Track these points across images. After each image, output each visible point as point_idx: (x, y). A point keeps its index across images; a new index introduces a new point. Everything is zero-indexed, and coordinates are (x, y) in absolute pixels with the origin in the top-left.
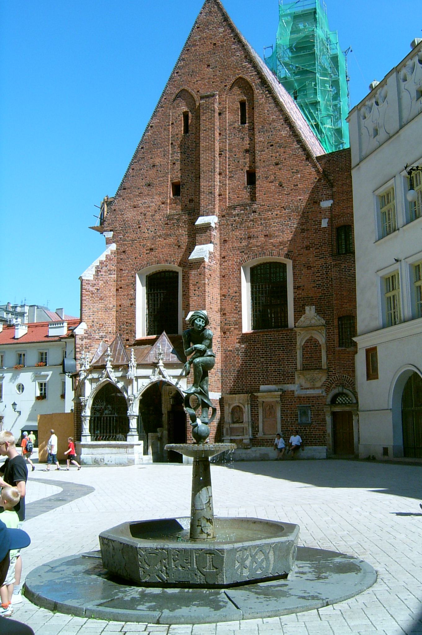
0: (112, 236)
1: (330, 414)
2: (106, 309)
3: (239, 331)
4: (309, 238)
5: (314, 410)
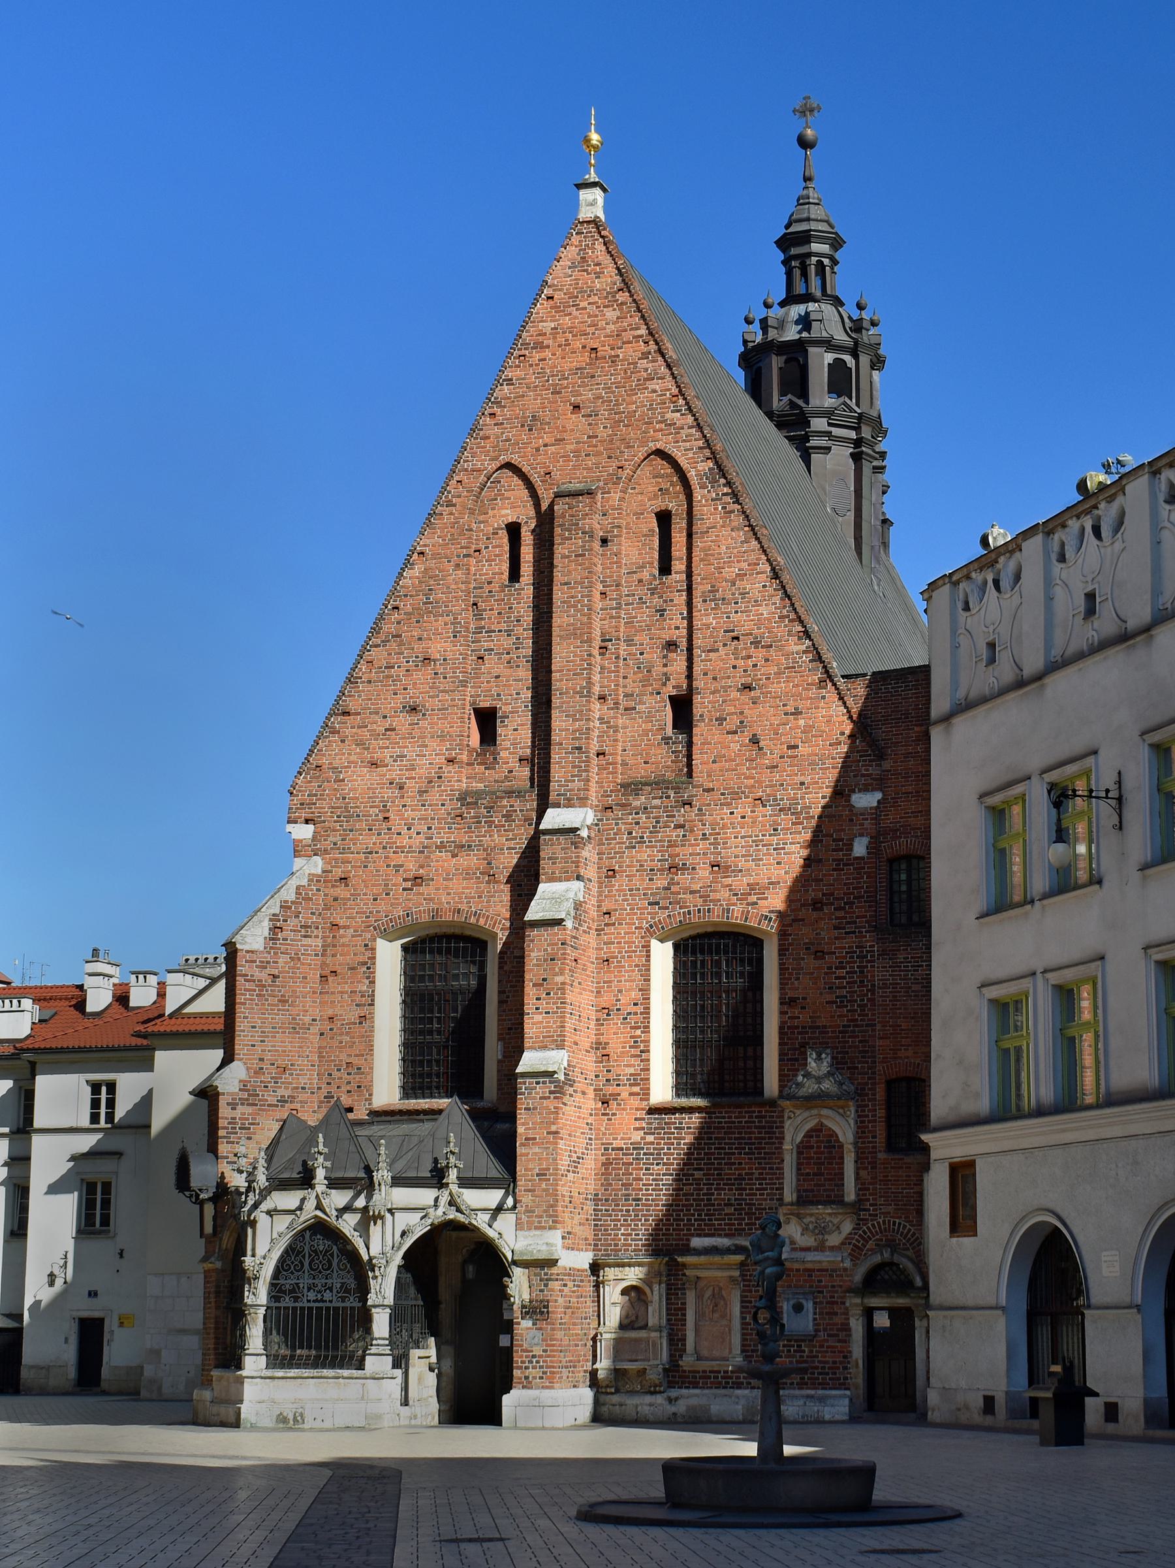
0: (310, 836)
1: (860, 1312)
2: (296, 1028)
3: (641, 1100)
5: (821, 1303)
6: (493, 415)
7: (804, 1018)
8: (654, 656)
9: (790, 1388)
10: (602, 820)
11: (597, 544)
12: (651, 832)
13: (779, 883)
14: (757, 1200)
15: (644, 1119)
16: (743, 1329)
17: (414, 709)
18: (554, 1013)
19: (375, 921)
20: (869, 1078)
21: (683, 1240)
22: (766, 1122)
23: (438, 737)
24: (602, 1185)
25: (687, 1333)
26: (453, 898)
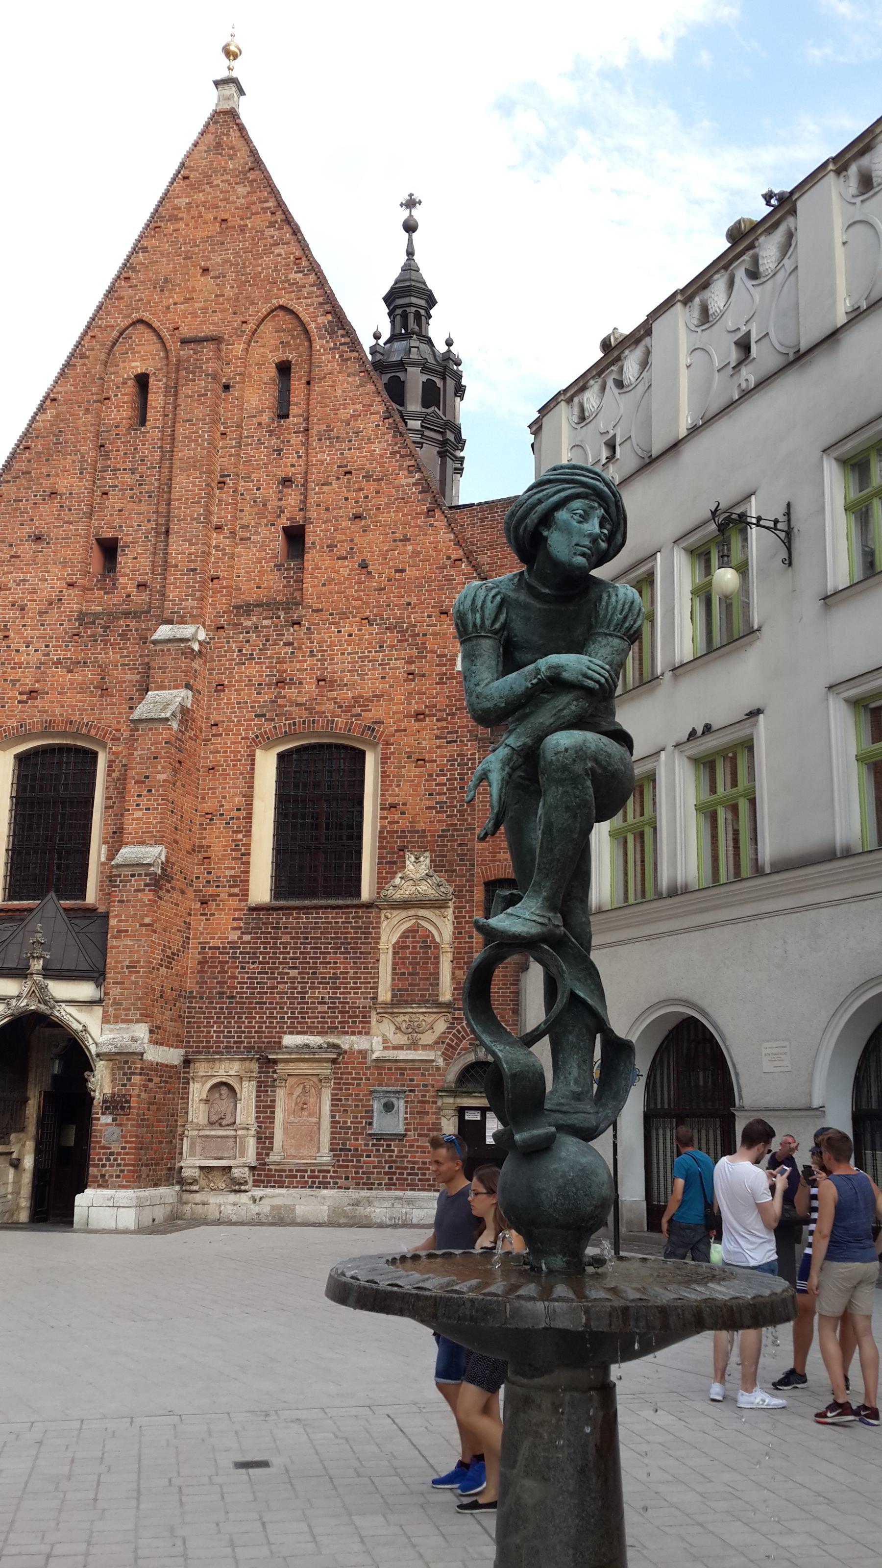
1: (451, 1112)
3: (240, 900)
4: (425, 693)
5: (412, 1102)
7: (403, 823)
8: (271, 492)
9: (376, 1189)
11: (220, 390)
12: (260, 650)
13: (382, 696)
14: (351, 998)
15: (242, 919)
16: (332, 1127)
17: (38, 538)
18: (154, 809)
20: (467, 881)
22: (363, 922)
23: (60, 563)
24: (197, 982)
25: (276, 1130)
26: (67, 711)
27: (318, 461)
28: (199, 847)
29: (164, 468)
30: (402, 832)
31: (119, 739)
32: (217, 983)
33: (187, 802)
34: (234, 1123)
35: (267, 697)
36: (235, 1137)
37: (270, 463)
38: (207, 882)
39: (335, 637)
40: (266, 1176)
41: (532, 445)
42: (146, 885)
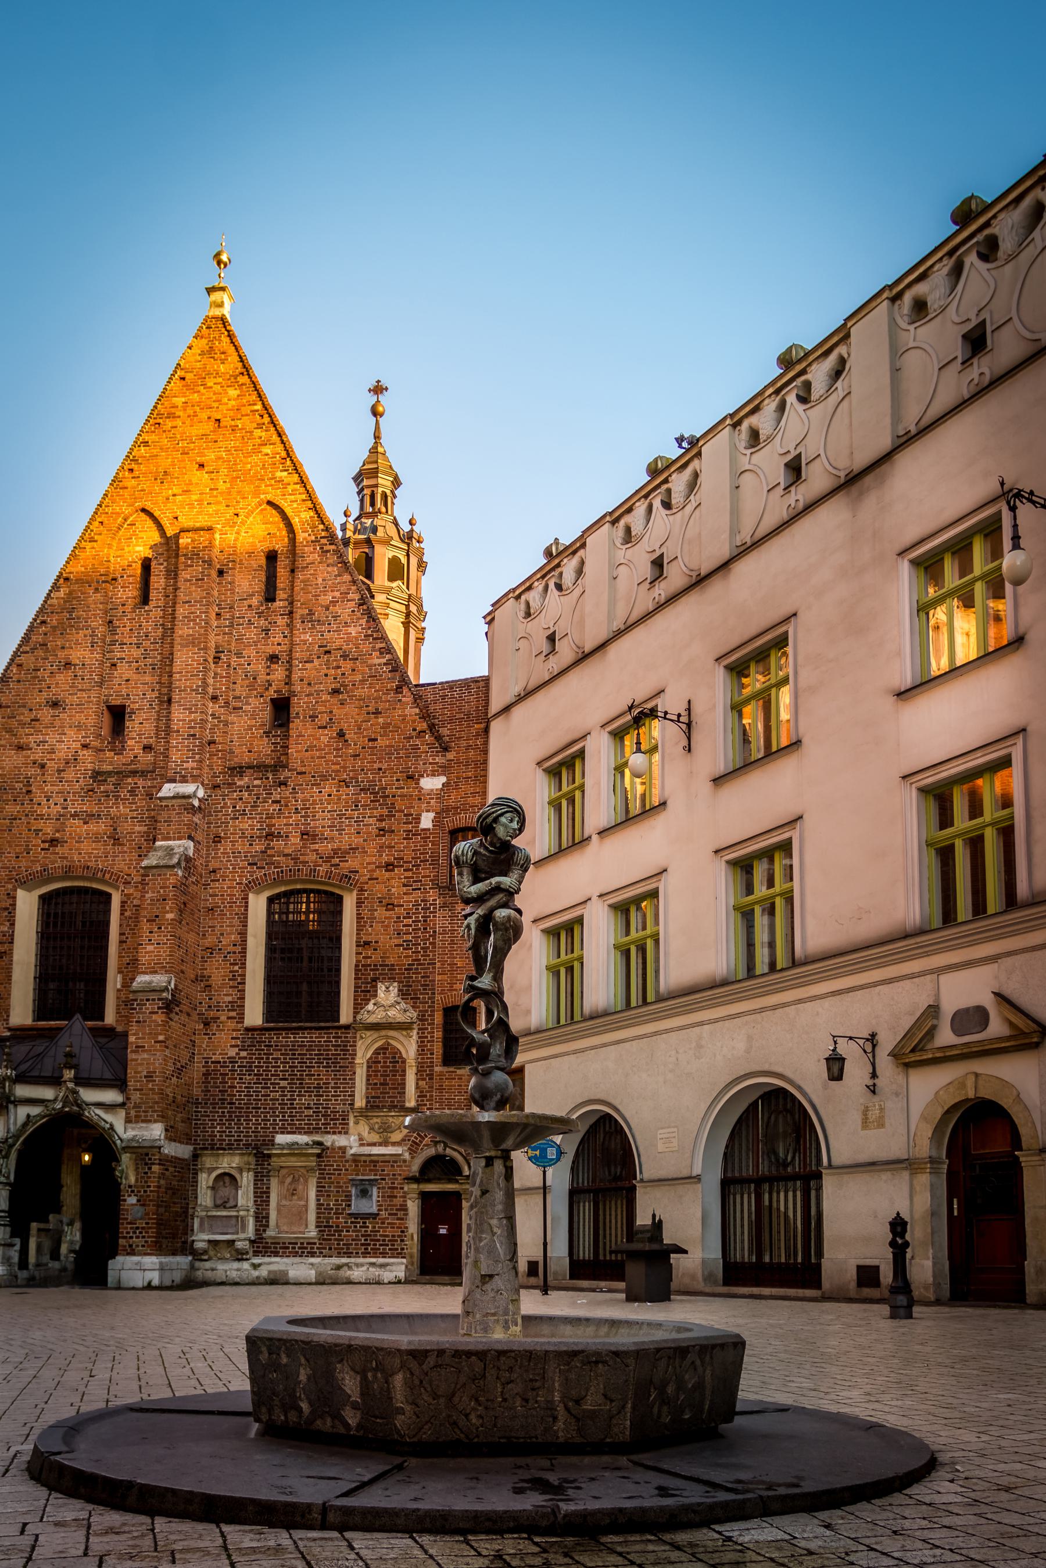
1: (416, 1196)
3: (237, 1022)
4: (394, 847)
5: (384, 1188)
6: (131, 470)
7: (376, 958)
8: (260, 667)
9: (355, 1257)
10: (211, 796)
11: (214, 574)
12: (252, 806)
13: (358, 848)
14: (332, 1104)
15: (239, 1038)
16: (317, 1209)
17: (55, 704)
19: (17, 875)
20: (429, 1007)
21: (269, 1136)
22: (342, 1042)
23: (75, 727)
24: (202, 1091)
26: (84, 857)
27: (302, 641)
28: (201, 977)
29: (166, 644)
30: (375, 965)
31: (130, 883)
32: (220, 1091)
33: (191, 937)
34: (236, 1206)
35: (258, 848)
36: (237, 1217)
37: (259, 642)
38: (209, 1007)
39: (317, 796)
40: (263, 1247)
41: (486, 634)
42: (159, 1008)
